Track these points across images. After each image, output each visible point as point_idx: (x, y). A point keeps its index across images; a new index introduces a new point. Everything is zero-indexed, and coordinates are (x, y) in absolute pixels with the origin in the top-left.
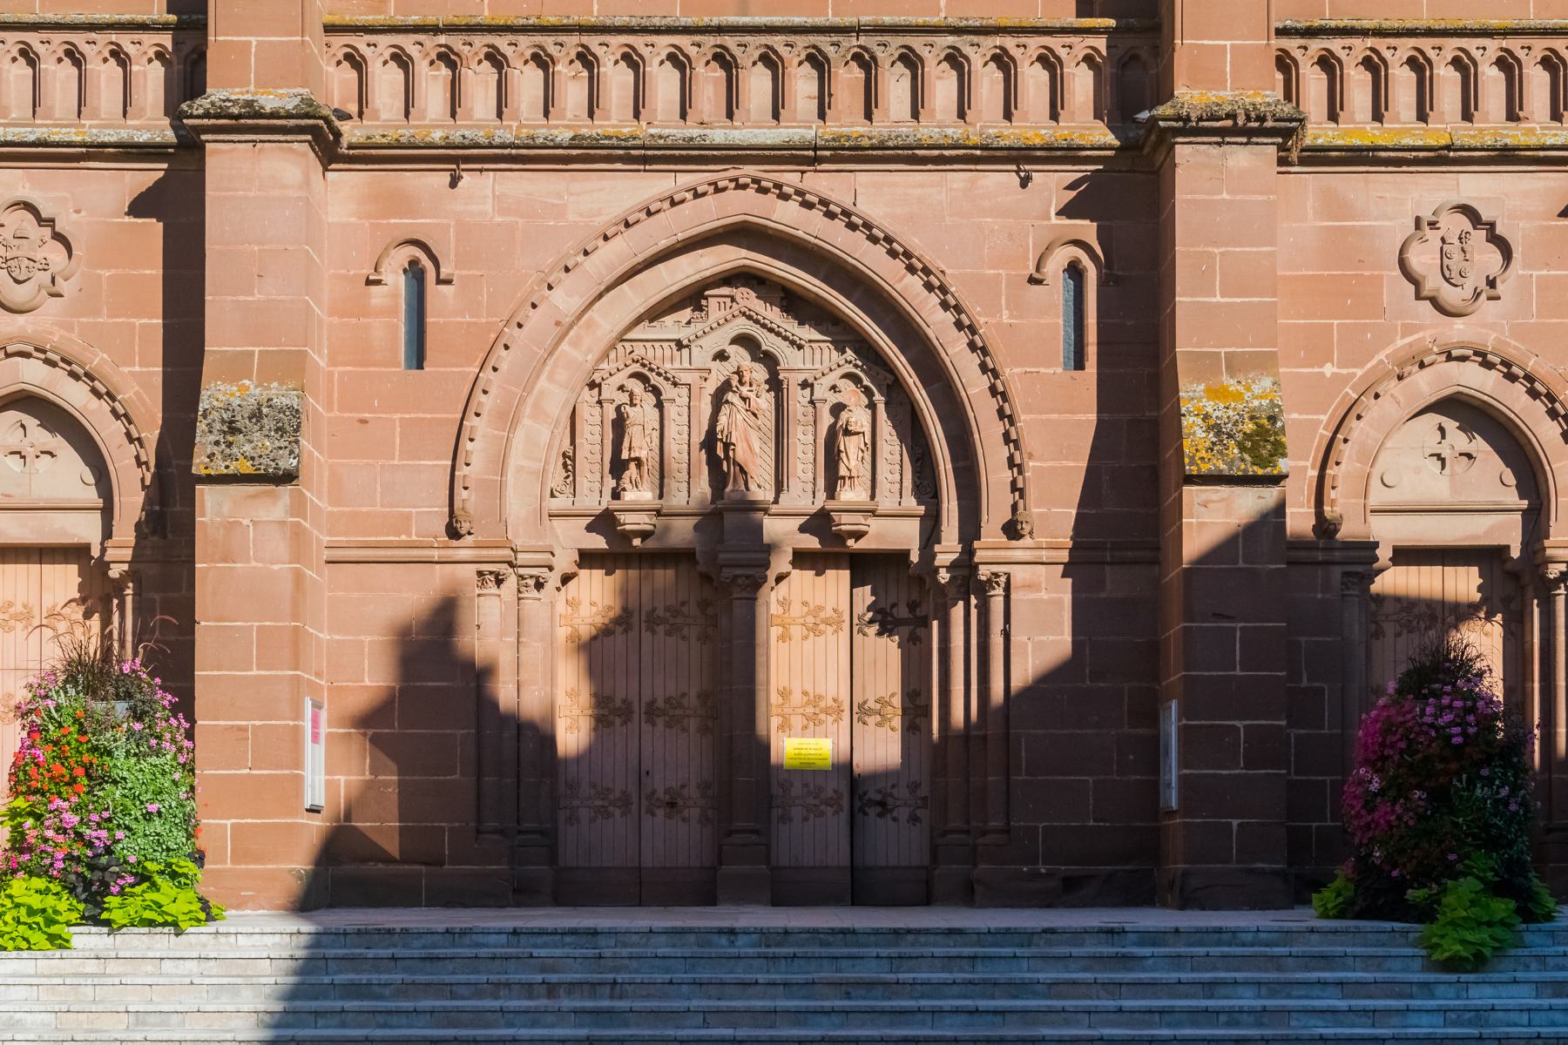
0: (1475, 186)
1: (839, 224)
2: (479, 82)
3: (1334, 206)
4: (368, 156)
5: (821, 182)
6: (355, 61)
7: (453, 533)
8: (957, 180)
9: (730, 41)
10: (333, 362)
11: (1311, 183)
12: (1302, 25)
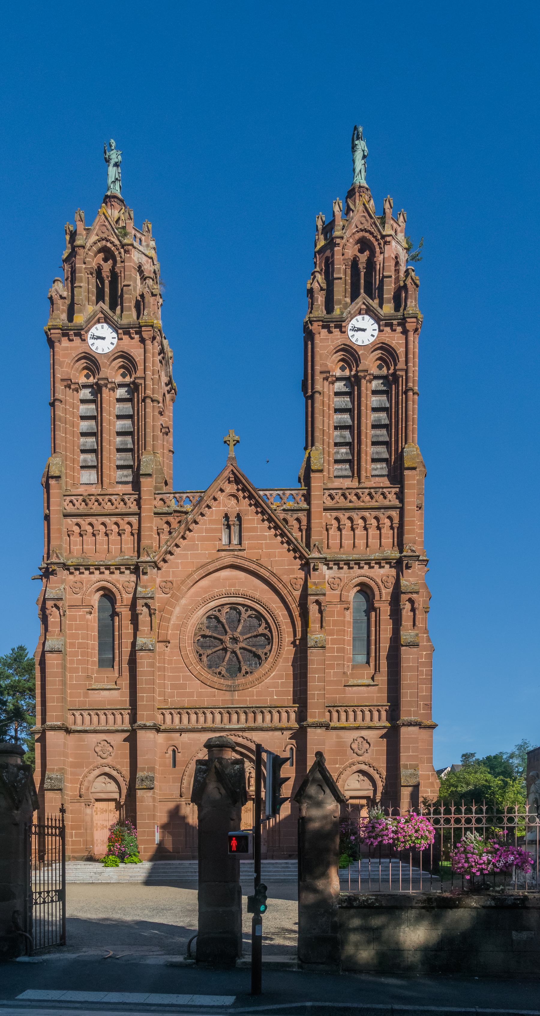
0: (364, 733)
1: (249, 741)
2: (185, 718)
3: (338, 737)
4: (165, 731)
5: (246, 734)
6: (163, 714)
7: (181, 796)
8: (270, 733)
9: (229, 710)
10: (160, 766)
11: (334, 732)
12: (333, 705)
